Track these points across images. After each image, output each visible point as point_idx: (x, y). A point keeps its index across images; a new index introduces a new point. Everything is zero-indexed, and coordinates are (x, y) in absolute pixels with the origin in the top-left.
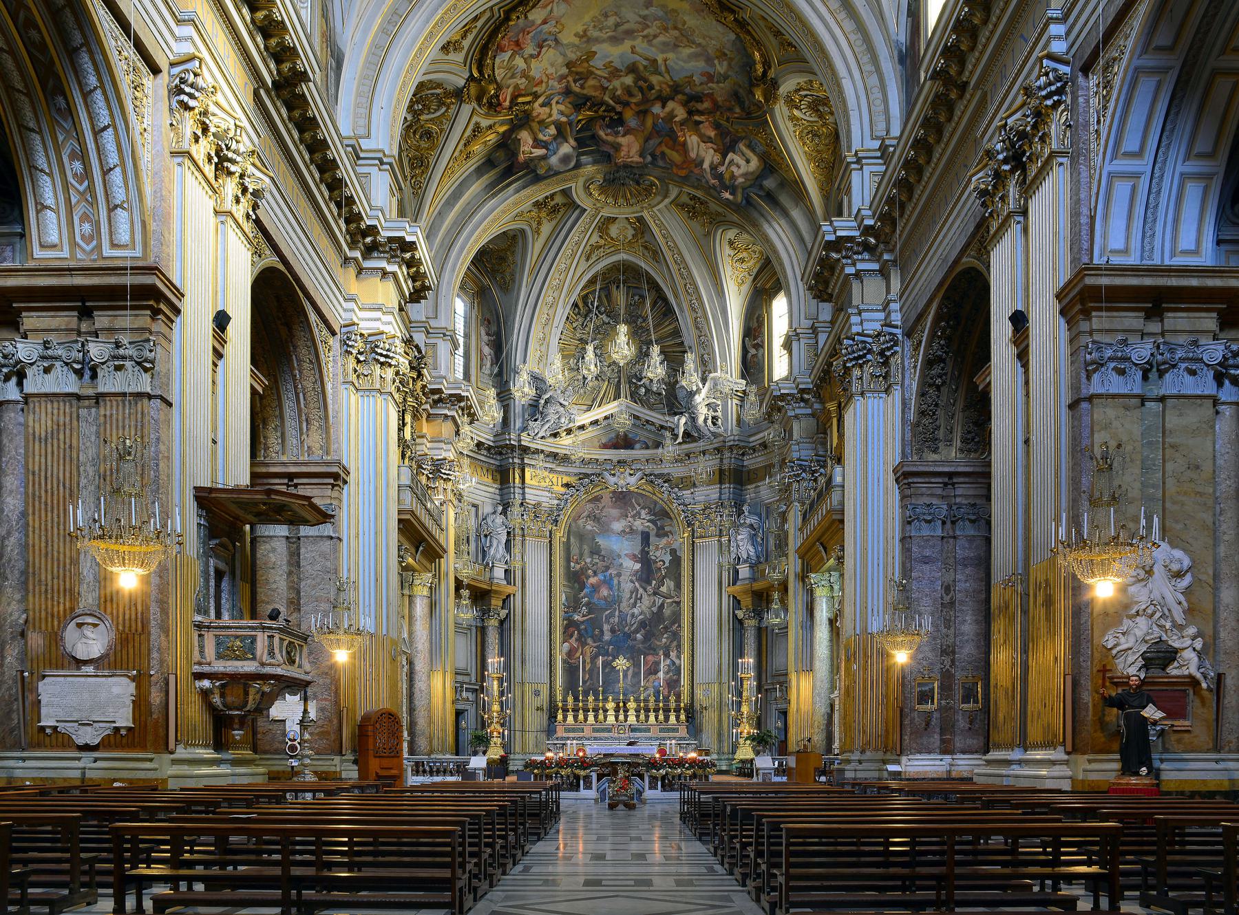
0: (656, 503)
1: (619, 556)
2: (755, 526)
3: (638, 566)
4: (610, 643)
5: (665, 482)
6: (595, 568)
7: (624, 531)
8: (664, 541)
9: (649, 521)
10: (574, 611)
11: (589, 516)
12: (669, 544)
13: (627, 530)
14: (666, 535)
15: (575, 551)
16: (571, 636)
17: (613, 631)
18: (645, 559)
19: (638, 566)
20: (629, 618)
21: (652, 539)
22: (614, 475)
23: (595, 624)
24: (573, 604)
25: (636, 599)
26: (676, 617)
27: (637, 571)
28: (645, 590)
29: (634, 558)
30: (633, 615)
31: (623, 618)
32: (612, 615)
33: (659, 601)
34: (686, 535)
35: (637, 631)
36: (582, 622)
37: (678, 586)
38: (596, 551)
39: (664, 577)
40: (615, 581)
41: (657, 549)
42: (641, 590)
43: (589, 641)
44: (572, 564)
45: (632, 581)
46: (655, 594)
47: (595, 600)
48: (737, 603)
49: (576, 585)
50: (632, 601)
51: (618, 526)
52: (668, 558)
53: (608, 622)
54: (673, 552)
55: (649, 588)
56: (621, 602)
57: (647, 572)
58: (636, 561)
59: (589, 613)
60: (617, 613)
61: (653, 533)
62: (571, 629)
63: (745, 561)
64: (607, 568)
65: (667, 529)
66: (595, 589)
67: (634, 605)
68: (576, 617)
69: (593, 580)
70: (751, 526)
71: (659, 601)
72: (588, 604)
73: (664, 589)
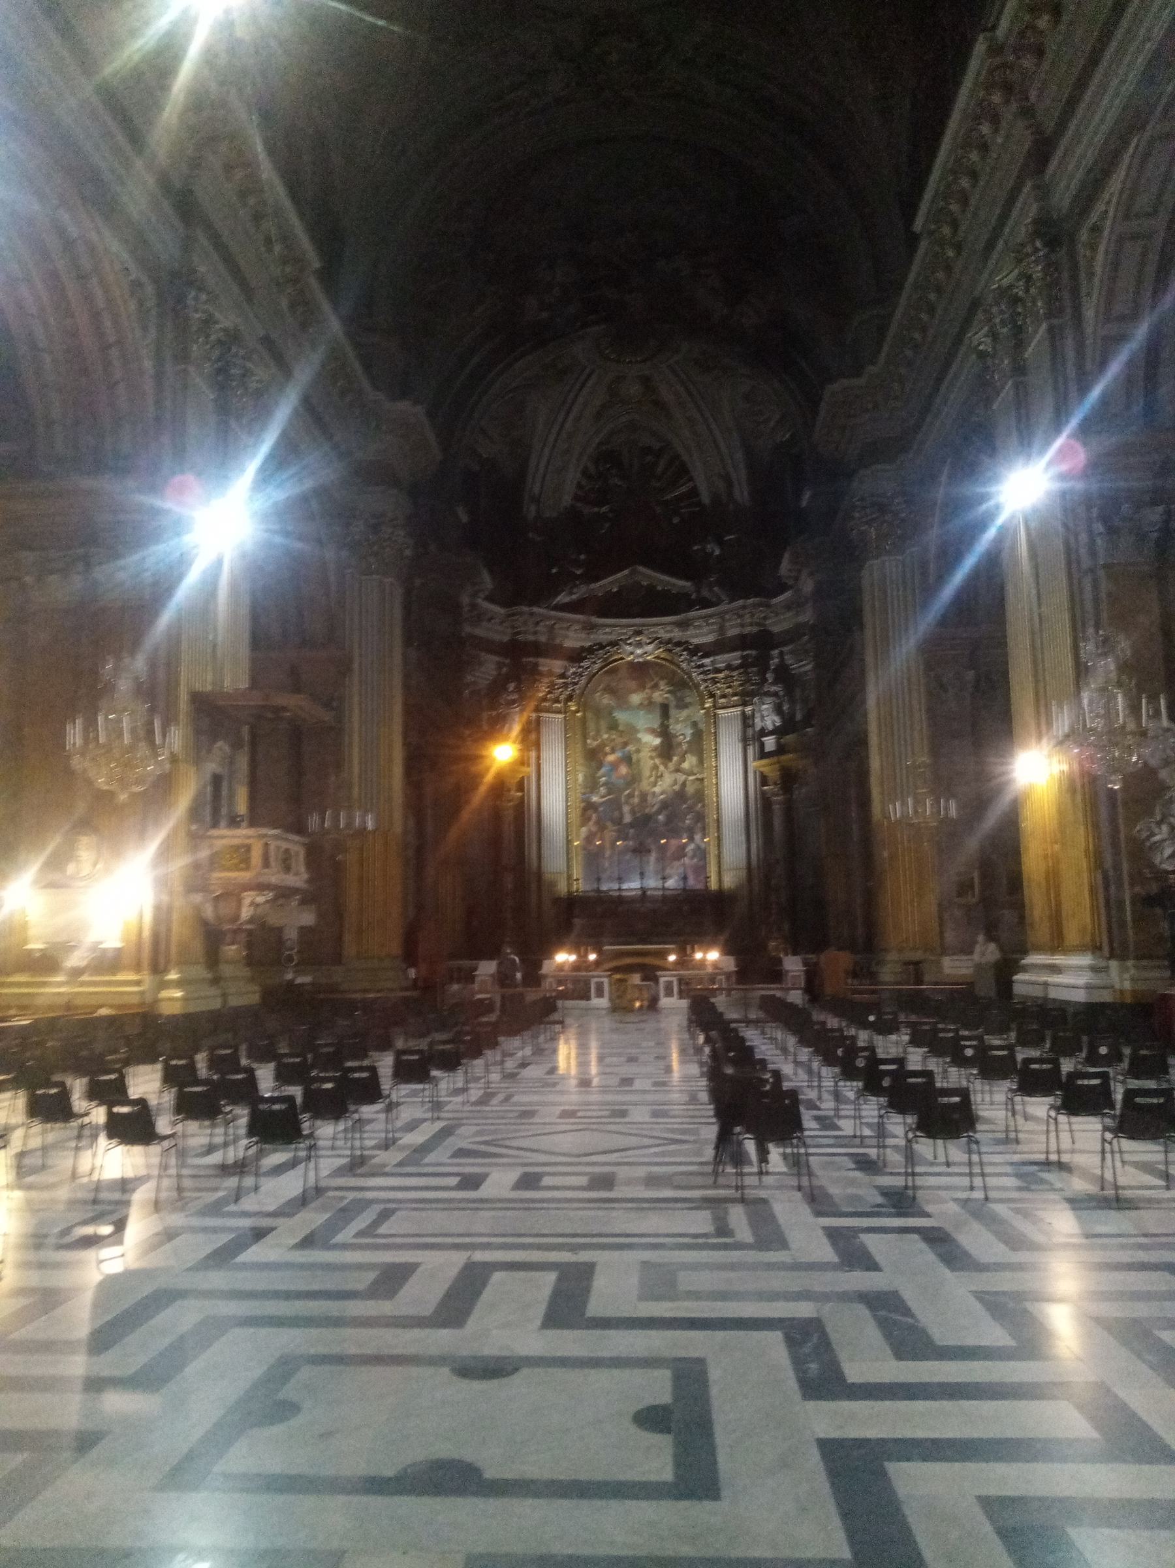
0: (674, 673)
1: (637, 731)
2: (781, 693)
3: (657, 741)
4: (631, 825)
5: (683, 651)
6: (612, 744)
7: (641, 704)
8: (685, 713)
9: (669, 692)
10: (592, 792)
11: (604, 690)
12: (688, 717)
13: (646, 702)
14: (686, 706)
15: (591, 726)
16: (589, 819)
17: (633, 812)
18: (664, 732)
19: (657, 741)
20: (649, 798)
21: (673, 712)
22: (630, 644)
23: (615, 804)
24: (592, 784)
25: (657, 777)
26: (700, 796)
27: (655, 749)
28: (666, 767)
29: (652, 731)
30: (654, 793)
31: (644, 797)
32: (631, 796)
33: (681, 777)
34: (707, 705)
35: (659, 812)
36: (602, 803)
37: (701, 761)
38: (613, 726)
39: (686, 752)
40: (634, 757)
41: (677, 722)
42: (662, 768)
43: (609, 824)
44: (589, 741)
45: (652, 758)
46: (677, 770)
47: (614, 778)
48: (764, 780)
49: (594, 764)
50: (652, 779)
51: (636, 698)
52: (689, 732)
53: (627, 803)
54: (695, 724)
55: (671, 766)
56: (640, 781)
57: (667, 750)
58: (657, 736)
59: (609, 794)
60: (636, 793)
61: (673, 704)
62: (589, 812)
63: (771, 733)
64: (626, 744)
65: (688, 700)
66: (615, 766)
67: (655, 784)
68: (595, 799)
69: (611, 758)
70: (775, 694)
71: (681, 777)
72: (605, 784)
73: (686, 765)
